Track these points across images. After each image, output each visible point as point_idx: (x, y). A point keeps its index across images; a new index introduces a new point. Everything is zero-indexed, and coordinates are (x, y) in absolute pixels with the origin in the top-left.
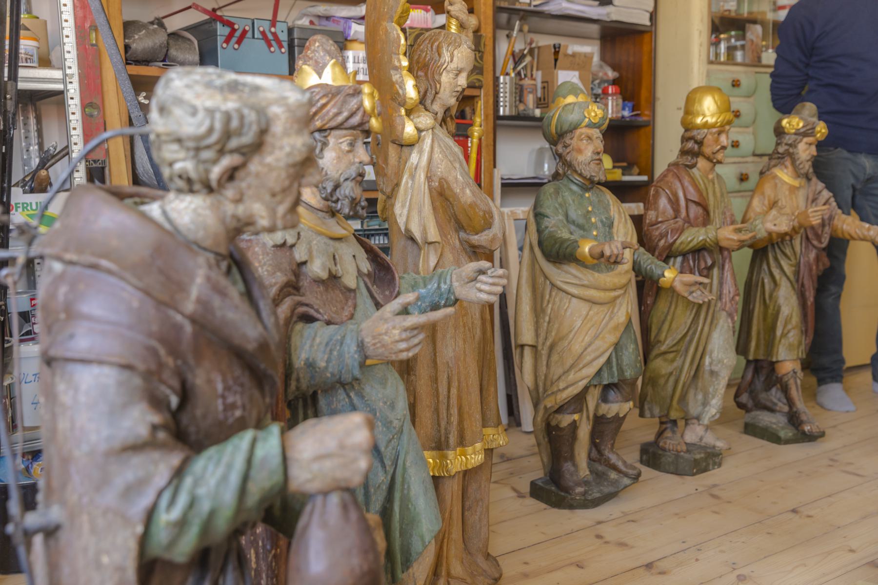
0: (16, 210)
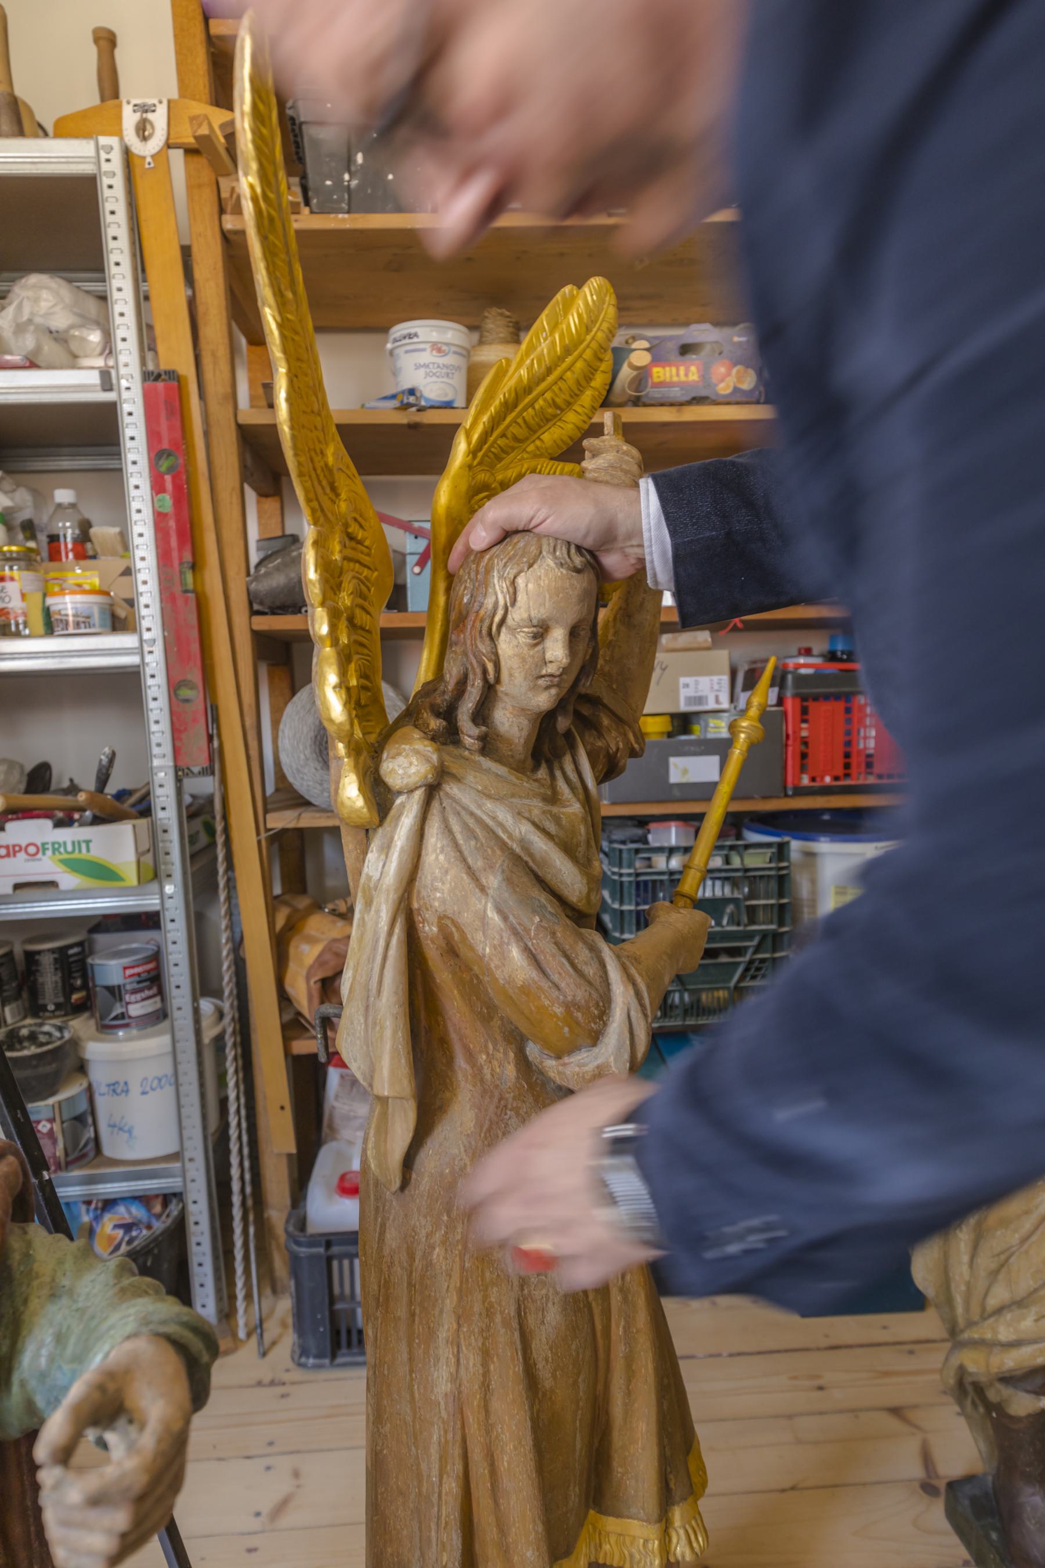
0: (44, 854)
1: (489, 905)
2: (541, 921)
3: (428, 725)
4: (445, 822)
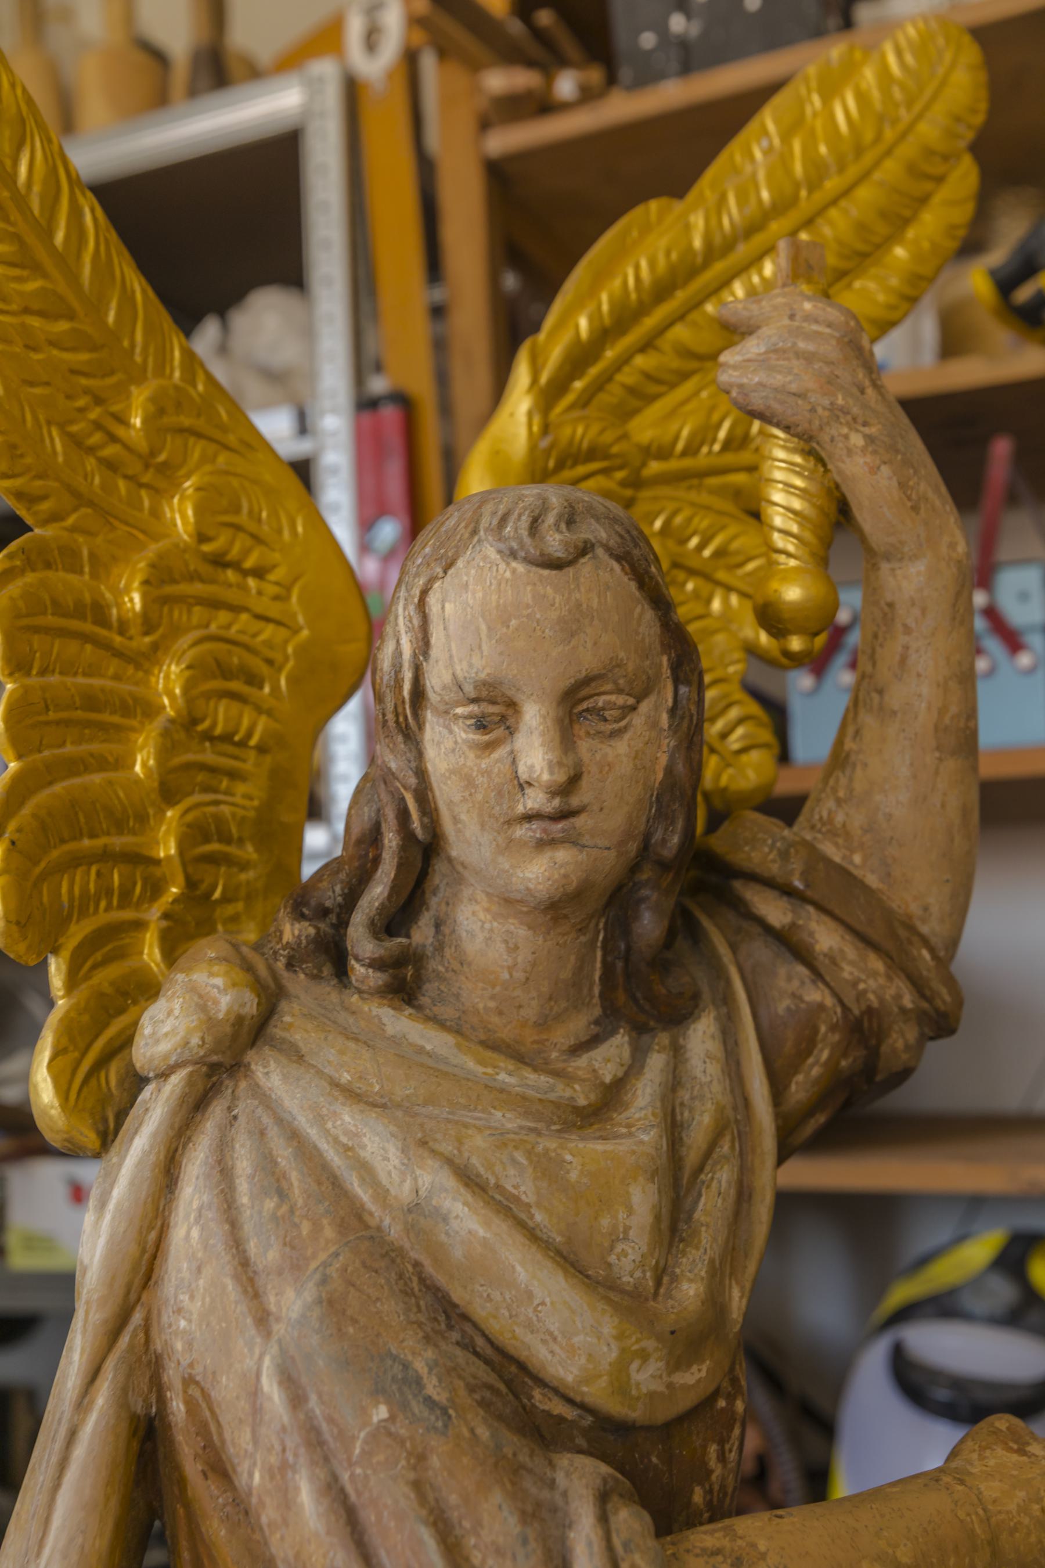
1: (267, 1361)
2: (392, 1418)
3: (281, 933)
4: (223, 1148)
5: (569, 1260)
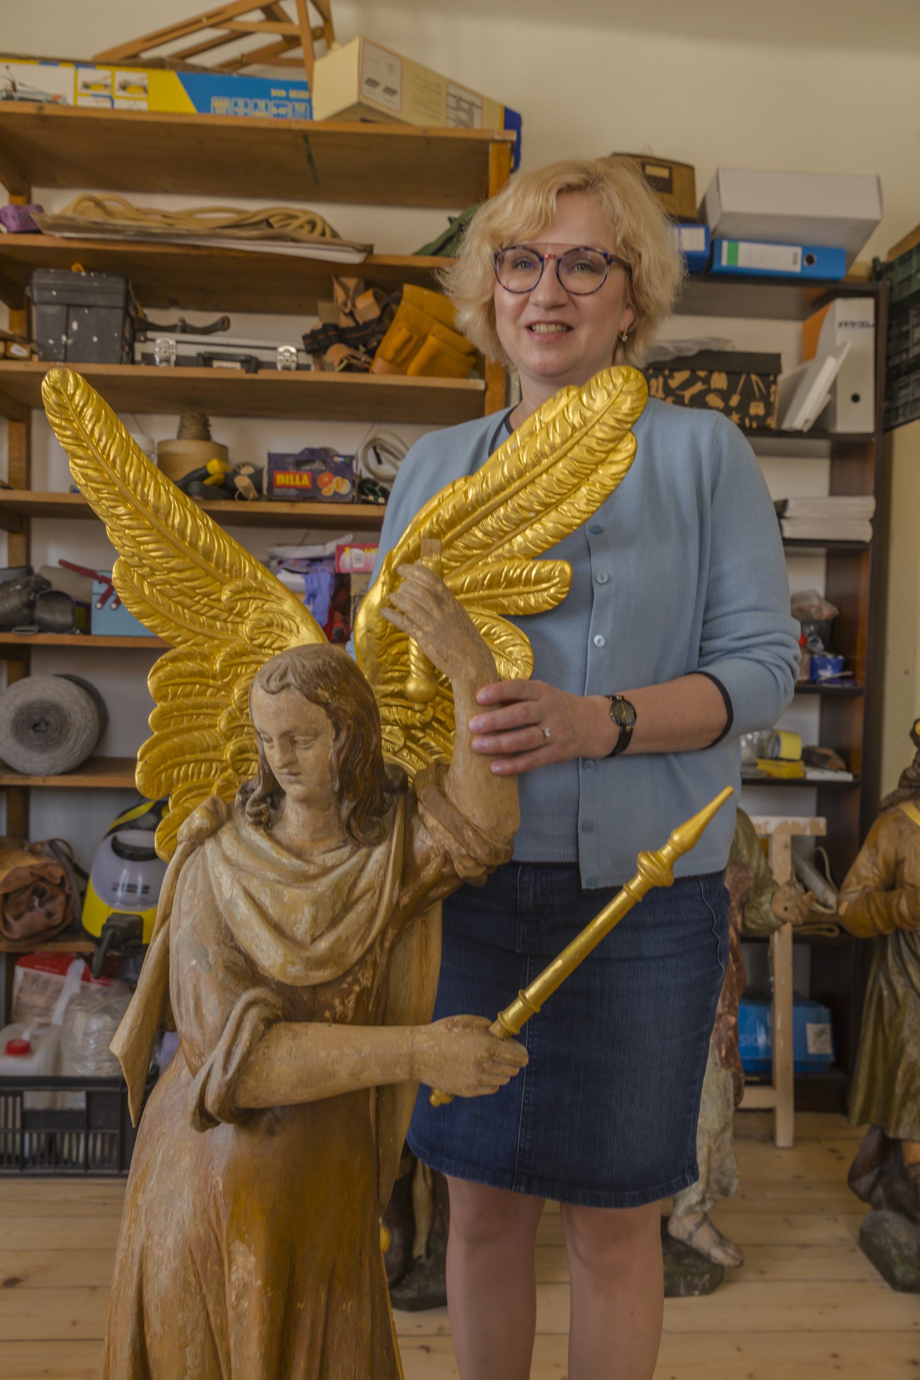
5: (277, 929)
